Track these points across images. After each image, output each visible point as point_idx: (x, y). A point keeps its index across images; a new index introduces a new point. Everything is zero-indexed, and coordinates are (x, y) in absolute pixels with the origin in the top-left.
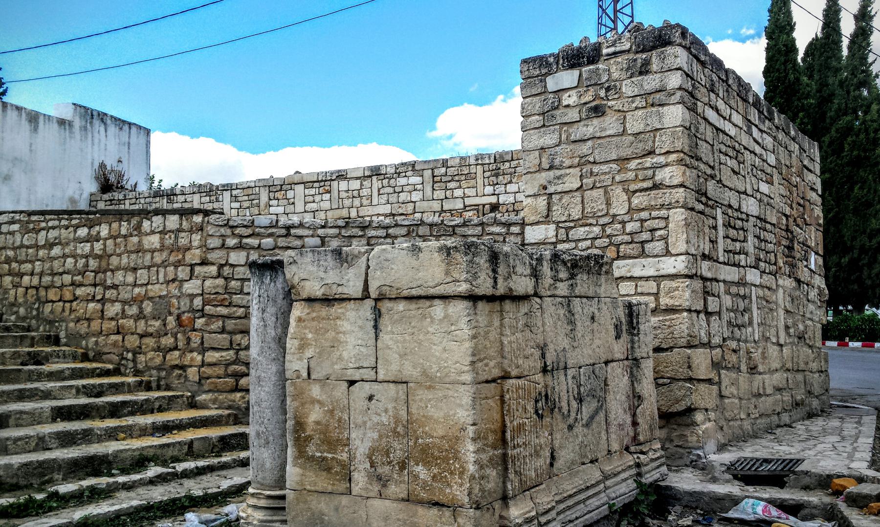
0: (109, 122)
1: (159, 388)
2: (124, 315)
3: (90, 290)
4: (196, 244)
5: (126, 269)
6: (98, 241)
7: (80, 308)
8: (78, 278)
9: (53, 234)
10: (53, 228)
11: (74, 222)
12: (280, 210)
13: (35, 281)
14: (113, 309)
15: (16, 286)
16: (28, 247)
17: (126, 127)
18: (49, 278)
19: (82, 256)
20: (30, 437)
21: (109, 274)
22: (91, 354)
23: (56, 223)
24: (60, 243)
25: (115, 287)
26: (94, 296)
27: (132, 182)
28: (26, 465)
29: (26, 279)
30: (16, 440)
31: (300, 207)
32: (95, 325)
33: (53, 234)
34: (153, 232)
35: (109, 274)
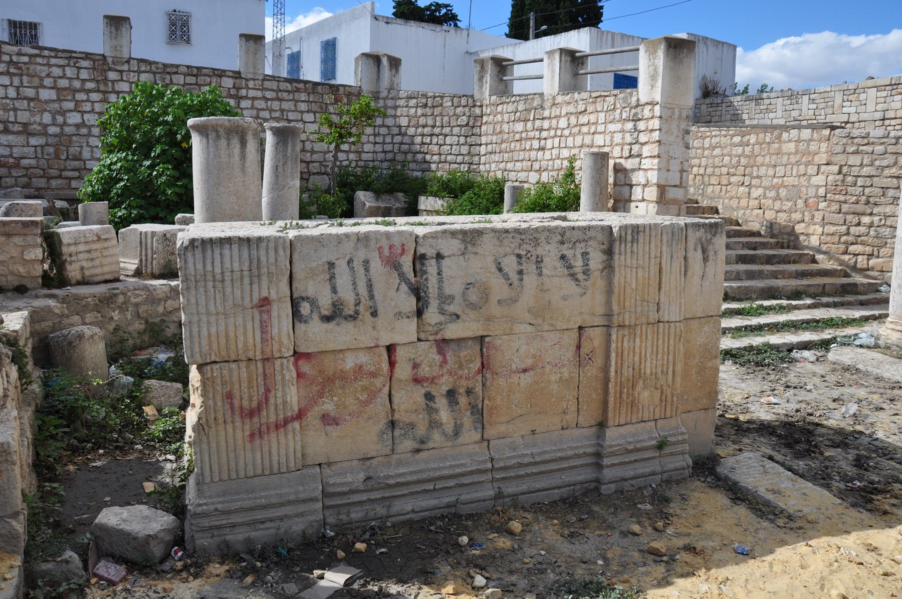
0: (709, 43)
1: (788, 247)
2: (765, 197)
3: (741, 178)
4: (823, 150)
5: (768, 166)
6: (748, 146)
7: (732, 190)
8: (732, 170)
9: (715, 140)
10: (715, 136)
11: (731, 132)
12: (853, 110)
13: (702, 171)
14: (756, 193)
16: (697, 149)
17: (720, 46)
18: (712, 169)
19: (736, 156)
20: (732, 271)
21: (755, 168)
22: (740, 222)
23: (718, 133)
24: (720, 146)
25: (759, 177)
26: (743, 183)
27: (723, 88)
28: (739, 287)
31: (871, 107)
33: (715, 140)
34: (790, 141)
35: (755, 168)
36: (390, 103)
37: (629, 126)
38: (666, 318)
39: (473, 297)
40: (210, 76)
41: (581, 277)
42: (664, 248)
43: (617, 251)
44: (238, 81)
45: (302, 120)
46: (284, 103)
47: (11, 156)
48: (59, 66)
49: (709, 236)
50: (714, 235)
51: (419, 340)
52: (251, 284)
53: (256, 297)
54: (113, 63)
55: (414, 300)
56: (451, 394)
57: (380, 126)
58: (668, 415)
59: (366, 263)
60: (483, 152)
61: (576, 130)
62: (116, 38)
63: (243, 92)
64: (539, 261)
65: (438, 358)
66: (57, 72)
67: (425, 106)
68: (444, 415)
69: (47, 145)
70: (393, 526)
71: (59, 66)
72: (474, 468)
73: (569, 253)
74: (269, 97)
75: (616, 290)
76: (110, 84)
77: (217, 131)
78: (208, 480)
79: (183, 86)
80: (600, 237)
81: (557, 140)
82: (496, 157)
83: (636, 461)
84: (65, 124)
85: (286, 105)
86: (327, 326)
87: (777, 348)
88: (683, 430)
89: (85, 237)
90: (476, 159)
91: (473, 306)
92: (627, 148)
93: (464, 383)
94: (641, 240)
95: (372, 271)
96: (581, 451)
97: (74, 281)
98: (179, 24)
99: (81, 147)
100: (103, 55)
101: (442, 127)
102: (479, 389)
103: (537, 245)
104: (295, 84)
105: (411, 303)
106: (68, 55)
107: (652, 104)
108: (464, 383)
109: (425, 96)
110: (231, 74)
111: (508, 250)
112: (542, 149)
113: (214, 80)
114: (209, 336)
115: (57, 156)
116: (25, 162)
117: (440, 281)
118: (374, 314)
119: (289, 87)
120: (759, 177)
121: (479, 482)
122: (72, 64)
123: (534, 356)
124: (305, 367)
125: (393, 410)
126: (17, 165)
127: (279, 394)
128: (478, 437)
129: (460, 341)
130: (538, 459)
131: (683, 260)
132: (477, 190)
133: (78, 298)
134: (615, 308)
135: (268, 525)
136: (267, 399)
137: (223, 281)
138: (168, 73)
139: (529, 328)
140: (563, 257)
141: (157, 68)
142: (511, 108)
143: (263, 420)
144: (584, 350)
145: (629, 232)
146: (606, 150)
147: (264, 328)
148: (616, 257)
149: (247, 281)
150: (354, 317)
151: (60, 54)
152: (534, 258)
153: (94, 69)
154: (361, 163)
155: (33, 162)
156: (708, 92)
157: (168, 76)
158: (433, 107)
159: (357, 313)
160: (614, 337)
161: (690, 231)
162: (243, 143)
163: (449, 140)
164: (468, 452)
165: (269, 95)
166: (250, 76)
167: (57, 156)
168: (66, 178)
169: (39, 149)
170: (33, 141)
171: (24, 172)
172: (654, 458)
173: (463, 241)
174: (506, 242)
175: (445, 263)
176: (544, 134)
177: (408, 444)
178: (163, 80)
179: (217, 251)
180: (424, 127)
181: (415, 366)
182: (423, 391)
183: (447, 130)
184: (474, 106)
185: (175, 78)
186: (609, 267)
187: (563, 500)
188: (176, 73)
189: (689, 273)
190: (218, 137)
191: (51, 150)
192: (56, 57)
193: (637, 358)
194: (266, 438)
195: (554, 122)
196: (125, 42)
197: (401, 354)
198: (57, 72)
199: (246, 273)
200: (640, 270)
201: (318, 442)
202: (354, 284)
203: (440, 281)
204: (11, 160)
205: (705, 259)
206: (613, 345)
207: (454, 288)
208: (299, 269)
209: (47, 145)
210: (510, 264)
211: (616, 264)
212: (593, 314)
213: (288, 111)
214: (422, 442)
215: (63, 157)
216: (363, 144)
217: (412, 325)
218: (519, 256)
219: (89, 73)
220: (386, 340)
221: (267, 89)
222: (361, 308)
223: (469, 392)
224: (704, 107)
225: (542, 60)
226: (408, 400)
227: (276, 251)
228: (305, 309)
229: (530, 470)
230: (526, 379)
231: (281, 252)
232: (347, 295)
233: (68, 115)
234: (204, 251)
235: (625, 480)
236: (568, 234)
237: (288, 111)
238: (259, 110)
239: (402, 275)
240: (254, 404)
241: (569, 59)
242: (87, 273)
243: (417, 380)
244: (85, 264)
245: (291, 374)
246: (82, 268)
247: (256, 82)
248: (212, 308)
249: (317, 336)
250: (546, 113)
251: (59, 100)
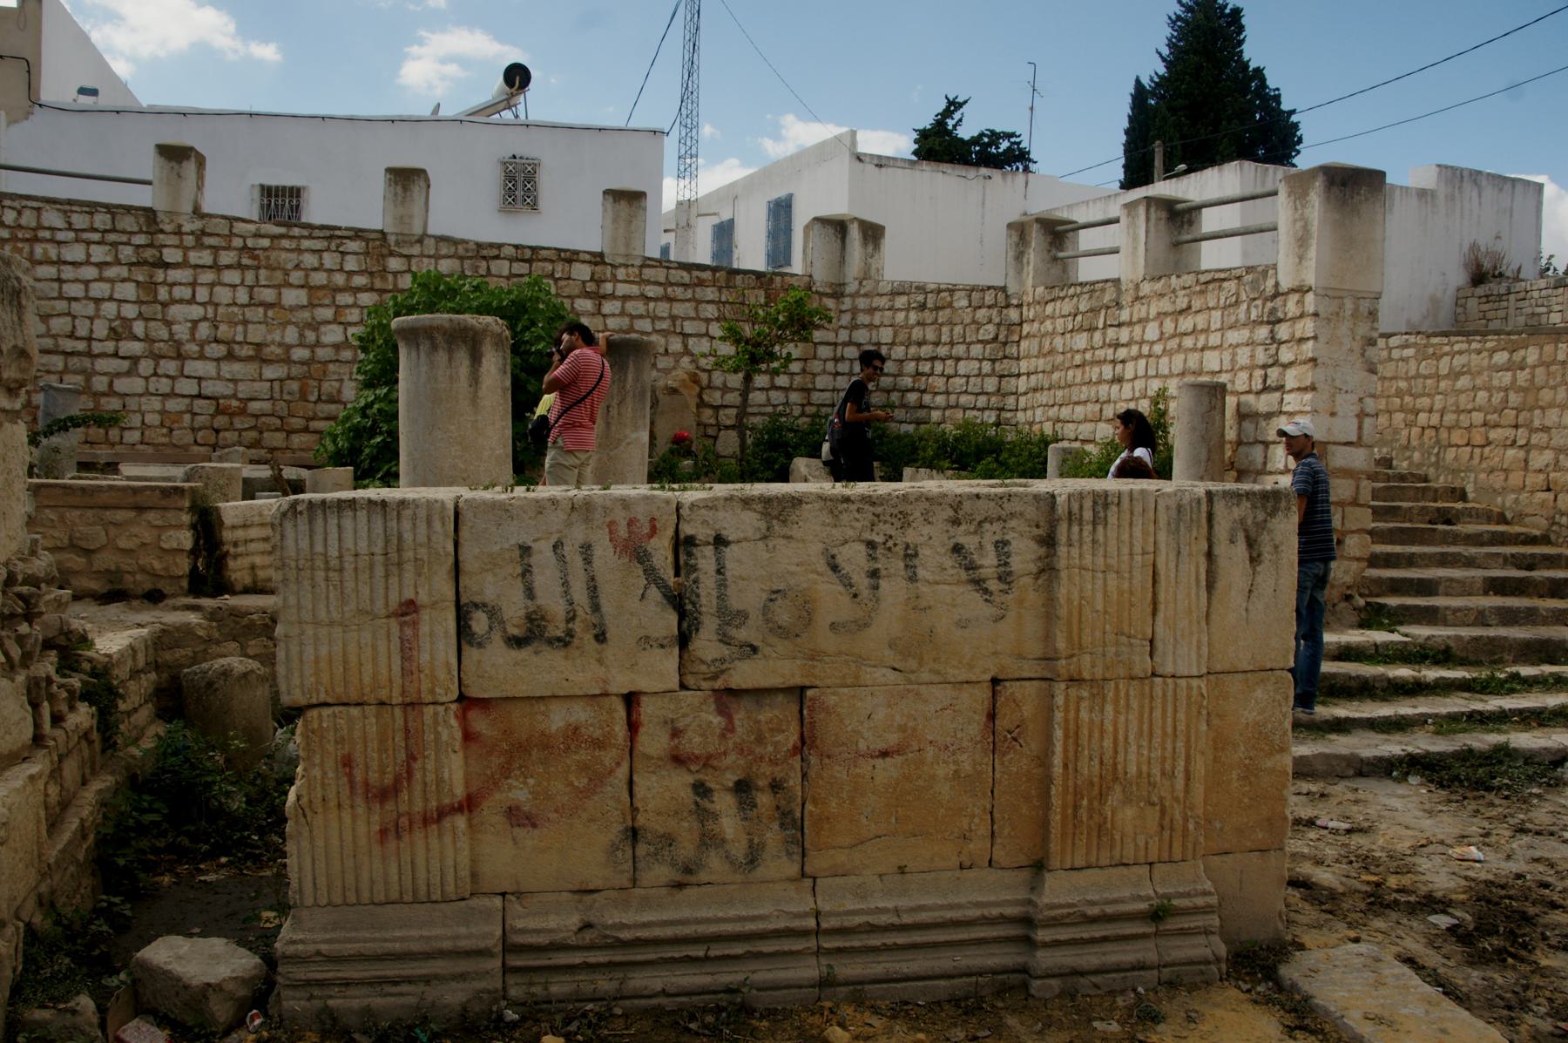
3: (1510, 432)
6: (1522, 369)
7: (1494, 456)
8: (1493, 417)
9: (1459, 361)
10: (1460, 353)
11: (1489, 345)
15: (1409, 425)
16: (1426, 377)
18: (1454, 416)
19: (1500, 389)
20: (1469, 609)
21: (1537, 412)
22: (1509, 515)
23: (1464, 346)
24: (1469, 372)
25: (1545, 429)
26: (1514, 442)
27: (1514, 266)
28: (1476, 639)
29: (1423, 418)
30: (1456, 610)
32: (1515, 479)
33: (1459, 361)
35: (1537, 412)
36: (862, 303)
37: (1263, 332)
38: (1169, 669)
39: (784, 615)
40: (552, 261)
41: (993, 585)
42: (1162, 537)
43: (1062, 536)
44: (599, 269)
45: (707, 334)
46: (676, 305)
47: (234, 396)
48: (314, 251)
49: (1261, 516)
50: (1273, 514)
51: (683, 686)
52: (387, 576)
53: (394, 599)
54: (397, 243)
55: (673, 618)
56: (743, 788)
57: (845, 344)
58: (1177, 855)
59: (586, 549)
60: (1022, 389)
61: (1173, 344)
62: (403, 202)
63: (608, 288)
64: (910, 555)
65: (717, 720)
66: (310, 260)
67: (922, 307)
68: (730, 824)
69: (289, 378)
70: (626, 1016)
71: (314, 251)
72: (782, 924)
73: (970, 542)
74: (650, 294)
75: (1063, 612)
76: (390, 277)
77: (432, 339)
78: (309, 901)
79: (508, 278)
80: (1031, 512)
81: (1142, 362)
82: (1043, 398)
83: (1105, 939)
84: (318, 343)
85: (679, 309)
86: (515, 654)
87: (1529, 757)
88: (1208, 886)
89: (261, 515)
90: (1011, 400)
91: (782, 632)
92: (1258, 373)
93: (766, 769)
94: (1112, 520)
95: (597, 563)
96: (995, 912)
97: (239, 587)
98: (520, 178)
99: (341, 381)
100: (382, 232)
101: (952, 344)
102: (794, 782)
103: (905, 525)
104: (696, 273)
105: (669, 621)
106: (328, 233)
107: (1301, 290)
108: (766, 769)
109: (921, 289)
110: (587, 257)
111: (850, 533)
112: (1118, 380)
113: (559, 267)
114: (317, 661)
115: (303, 397)
116: (254, 406)
117: (722, 585)
118: (601, 638)
119: (687, 279)
120: (1545, 429)
121: (791, 953)
122: (333, 247)
123: (902, 729)
124: (480, 723)
125: (634, 810)
126: (243, 412)
127: (430, 766)
128: (794, 869)
129: (760, 694)
130: (907, 919)
131: (1203, 561)
132: (1004, 455)
133: (236, 613)
134: (1061, 644)
135: (405, 988)
136: (410, 773)
137: (341, 570)
138: (484, 258)
139: (892, 676)
140: (957, 549)
141: (467, 250)
142: (1067, 306)
143: (403, 808)
144: (1002, 723)
145: (1088, 503)
146: (1224, 378)
147: (407, 651)
148: (1062, 550)
149: (379, 571)
150: (565, 641)
151: (317, 233)
152: (900, 549)
153: (367, 253)
154: (810, 410)
155: (267, 406)
156: (1483, 275)
157: (484, 263)
158: (937, 309)
159: (570, 633)
160: (1060, 700)
161: (1220, 508)
162: (476, 358)
163: (963, 367)
164: (775, 901)
165: (651, 291)
166: (620, 260)
167: (303, 397)
168: (315, 432)
169: (276, 385)
170: (270, 372)
171: (252, 422)
172: (1144, 936)
173: (765, 514)
174: (845, 517)
175: (730, 553)
176: (1122, 353)
177: (661, 872)
178: (476, 269)
179: (333, 521)
180: (920, 344)
181: (676, 733)
182: (690, 779)
183: (960, 350)
184: (1007, 306)
185: (496, 266)
186: (1047, 570)
187: (955, 1001)
188: (497, 257)
189: (1220, 585)
190: (434, 347)
191: (295, 386)
192: (310, 237)
193: (1108, 743)
194: (406, 838)
195: (1138, 329)
196: (417, 209)
197: (648, 709)
198: (310, 260)
199: (379, 559)
200: (1111, 576)
201: (503, 854)
202: (565, 584)
203: (722, 585)
204: (235, 403)
205: (1255, 560)
206: (1059, 716)
207: (748, 597)
208: (469, 553)
209: (289, 378)
210: (854, 558)
211: (1062, 564)
212: (1020, 657)
213: (684, 319)
214: (688, 870)
215: (313, 398)
216: (814, 375)
217: (669, 662)
218: (871, 545)
219: (359, 262)
220: (622, 682)
221: (648, 282)
222: (577, 626)
223: (776, 786)
224: (1472, 304)
225: (1117, 221)
226: (663, 790)
227: (429, 522)
228: (479, 623)
229: (890, 939)
230: (887, 770)
231: (437, 525)
232: (552, 601)
233: (323, 329)
234: (311, 522)
235: (1082, 974)
236: (967, 506)
237: (684, 319)
238: (632, 317)
239: (651, 574)
240: (388, 779)
241: (1164, 215)
242: (261, 574)
243: (678, 760)
244: (258, 560)
245: (451, 730)
246: (253, 567)
247: (630, 270)
248: (322, 615)
249: (499, 668)
250: (1125, 315)
251: (311, 305)
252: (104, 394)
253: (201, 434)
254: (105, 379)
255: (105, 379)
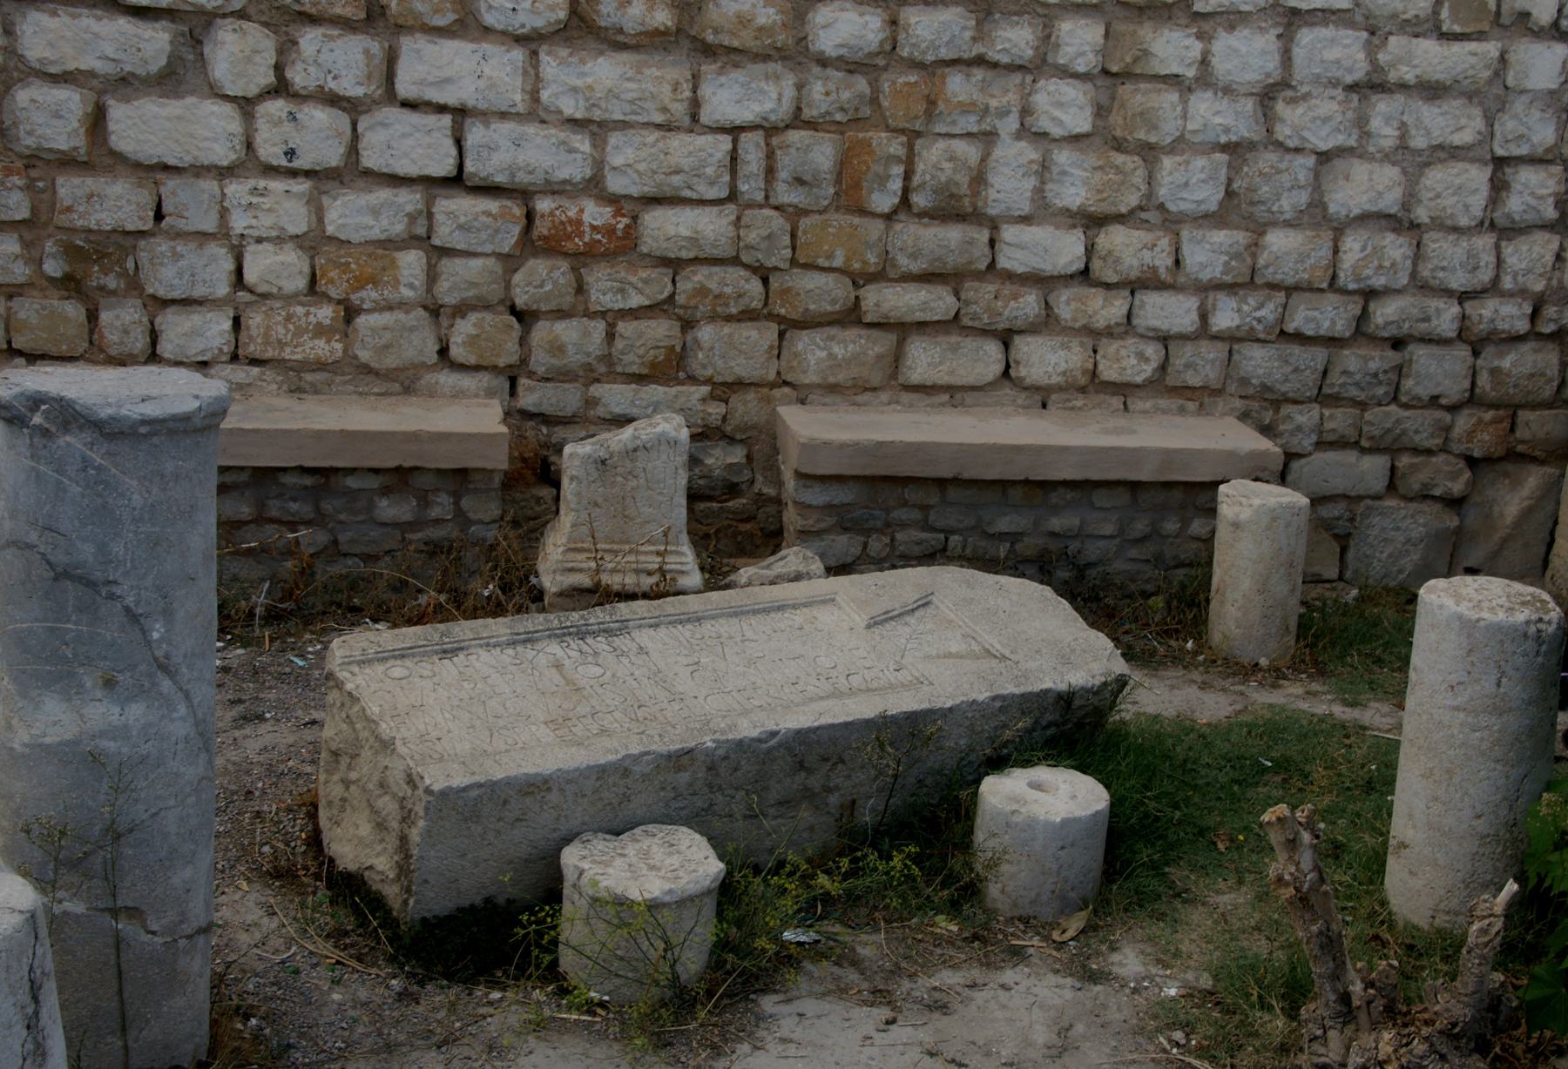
47: (594, 186)
69: (797, 121)
115: (849, 194)
116: (667, 228)
126: (622, 246)
155: (711, 226)
169: (752, 150)
170: (733, 97)
171: (657, 285)
191: (822, 153)
204: (594, 213)
209: (797, 121)
215: (883, 201)
252: (67, 162)
253: (464, 329)
254: (72, 101)
255: (72, 101)
